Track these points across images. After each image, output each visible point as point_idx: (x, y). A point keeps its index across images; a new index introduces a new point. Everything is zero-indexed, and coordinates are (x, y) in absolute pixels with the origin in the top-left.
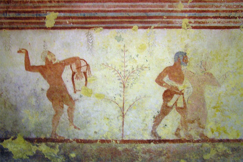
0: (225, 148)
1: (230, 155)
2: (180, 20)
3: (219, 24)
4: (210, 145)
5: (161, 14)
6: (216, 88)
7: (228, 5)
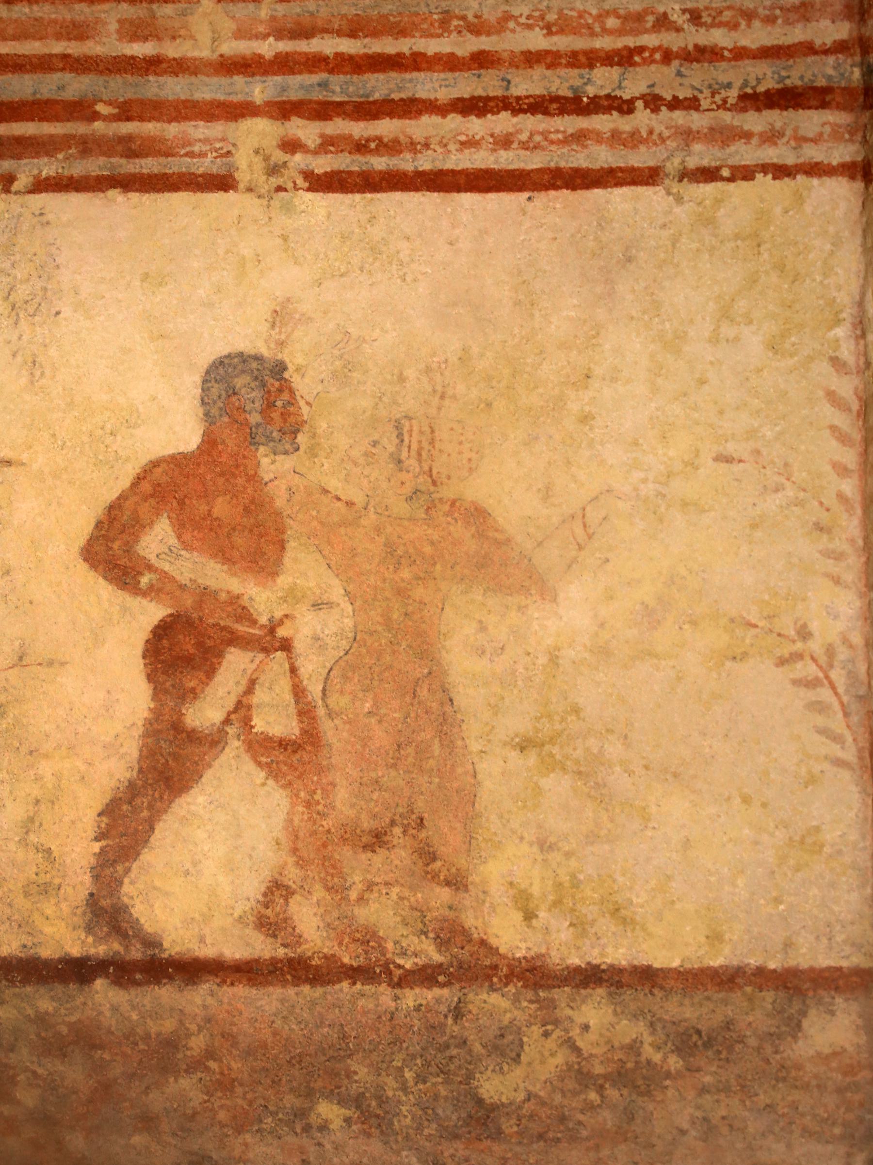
0: (630, 1030)
1: (668, 1075)
2: (217, 129)
3: (502, 152)
4: (516, 1000)
5: (75, 86)
6: (521, 609)
7: (560, 12)
